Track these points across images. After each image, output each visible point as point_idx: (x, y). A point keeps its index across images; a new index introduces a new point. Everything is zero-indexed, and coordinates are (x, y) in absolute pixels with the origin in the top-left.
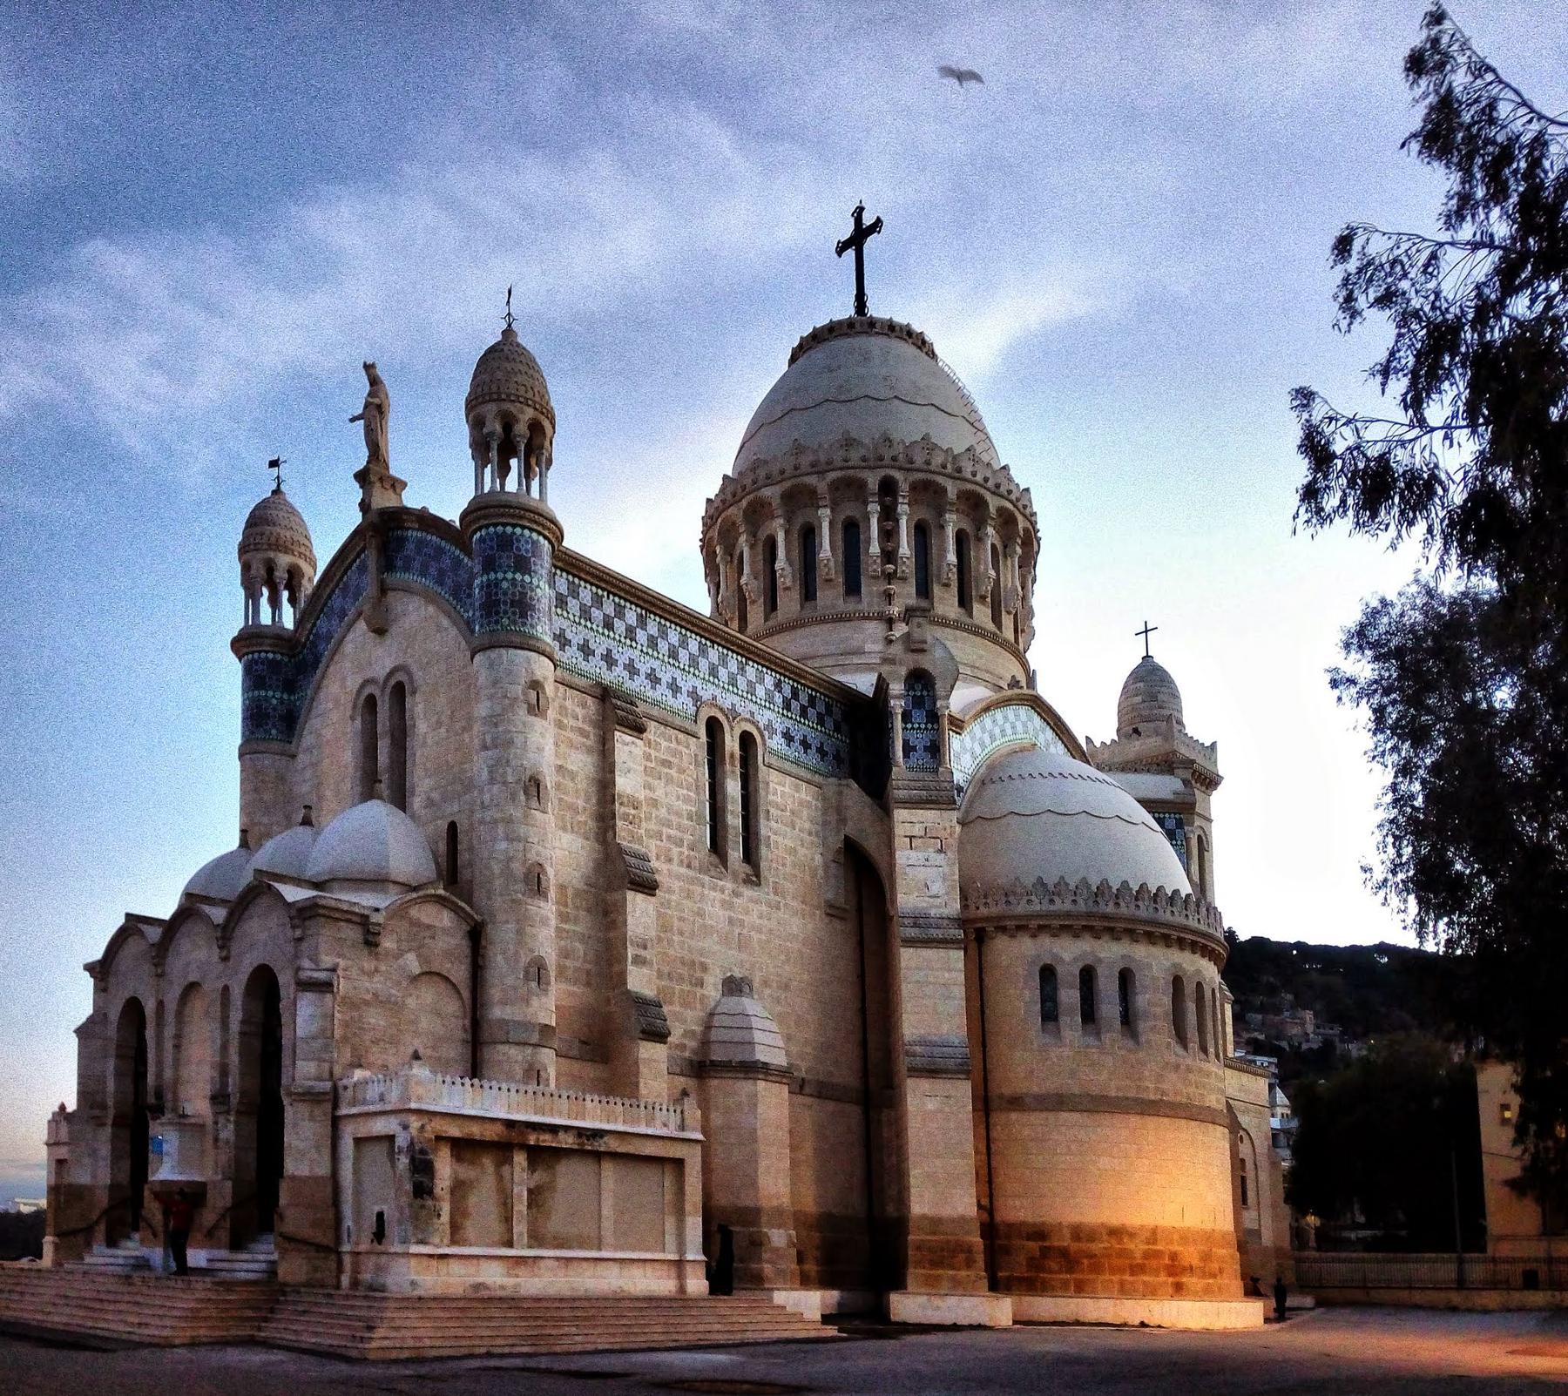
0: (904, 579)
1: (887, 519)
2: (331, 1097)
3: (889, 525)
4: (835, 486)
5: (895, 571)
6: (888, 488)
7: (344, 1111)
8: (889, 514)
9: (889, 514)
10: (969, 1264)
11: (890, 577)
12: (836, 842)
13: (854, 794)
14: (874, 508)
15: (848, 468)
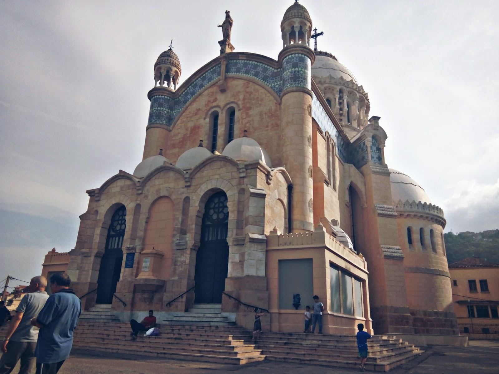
0: (344, 116)
1: (340, 99)
2: (265, 242)
3: (341, 101)
4: (325, 89)
5: (343, 113)
6: (341, 91)
7: (270, 248)
8: (341, 98)
9: (341, 98)
10: (407, 323)
11: (341, 115)
12: (348, 183)
13: (352, 169)
14: (337, 96)
15: (331, 84)
